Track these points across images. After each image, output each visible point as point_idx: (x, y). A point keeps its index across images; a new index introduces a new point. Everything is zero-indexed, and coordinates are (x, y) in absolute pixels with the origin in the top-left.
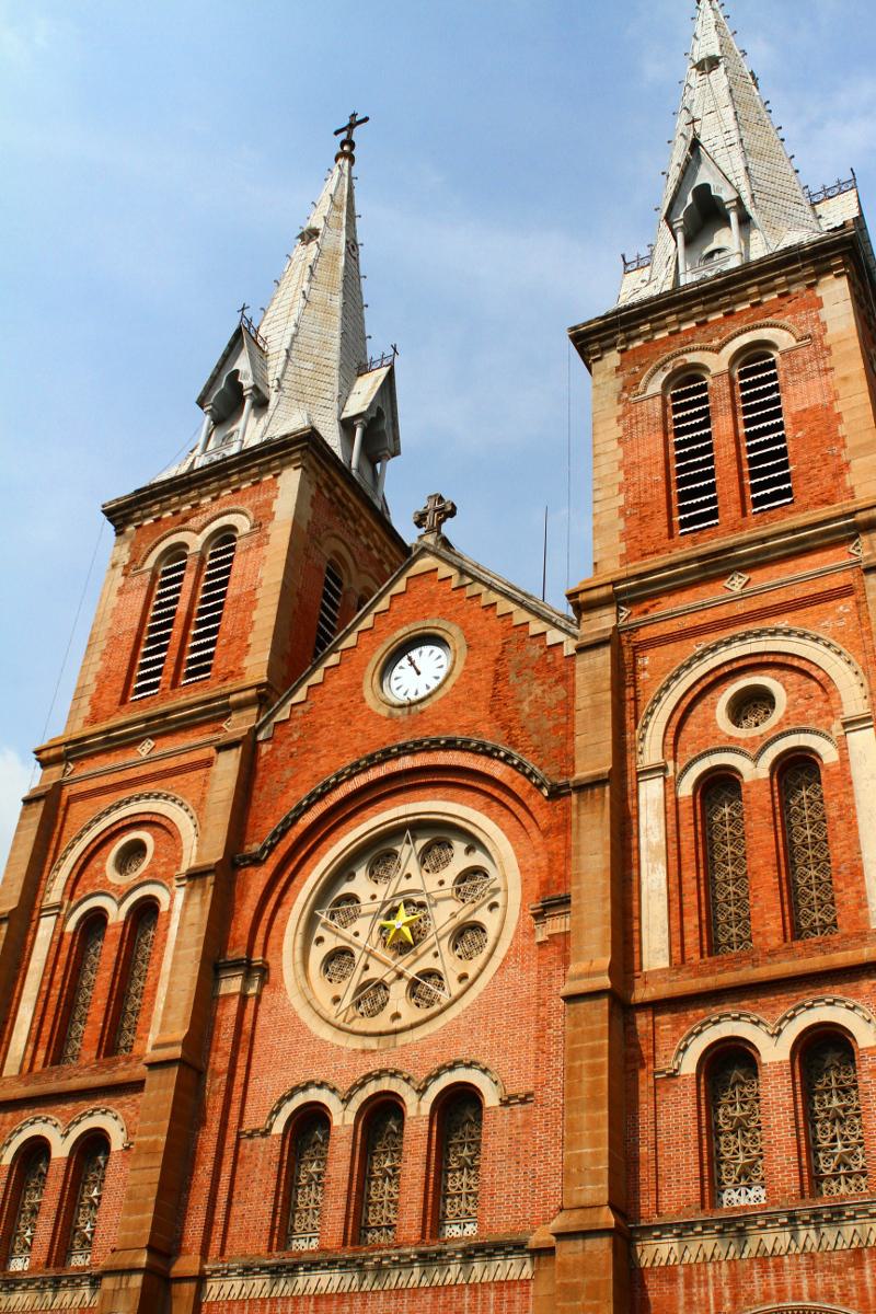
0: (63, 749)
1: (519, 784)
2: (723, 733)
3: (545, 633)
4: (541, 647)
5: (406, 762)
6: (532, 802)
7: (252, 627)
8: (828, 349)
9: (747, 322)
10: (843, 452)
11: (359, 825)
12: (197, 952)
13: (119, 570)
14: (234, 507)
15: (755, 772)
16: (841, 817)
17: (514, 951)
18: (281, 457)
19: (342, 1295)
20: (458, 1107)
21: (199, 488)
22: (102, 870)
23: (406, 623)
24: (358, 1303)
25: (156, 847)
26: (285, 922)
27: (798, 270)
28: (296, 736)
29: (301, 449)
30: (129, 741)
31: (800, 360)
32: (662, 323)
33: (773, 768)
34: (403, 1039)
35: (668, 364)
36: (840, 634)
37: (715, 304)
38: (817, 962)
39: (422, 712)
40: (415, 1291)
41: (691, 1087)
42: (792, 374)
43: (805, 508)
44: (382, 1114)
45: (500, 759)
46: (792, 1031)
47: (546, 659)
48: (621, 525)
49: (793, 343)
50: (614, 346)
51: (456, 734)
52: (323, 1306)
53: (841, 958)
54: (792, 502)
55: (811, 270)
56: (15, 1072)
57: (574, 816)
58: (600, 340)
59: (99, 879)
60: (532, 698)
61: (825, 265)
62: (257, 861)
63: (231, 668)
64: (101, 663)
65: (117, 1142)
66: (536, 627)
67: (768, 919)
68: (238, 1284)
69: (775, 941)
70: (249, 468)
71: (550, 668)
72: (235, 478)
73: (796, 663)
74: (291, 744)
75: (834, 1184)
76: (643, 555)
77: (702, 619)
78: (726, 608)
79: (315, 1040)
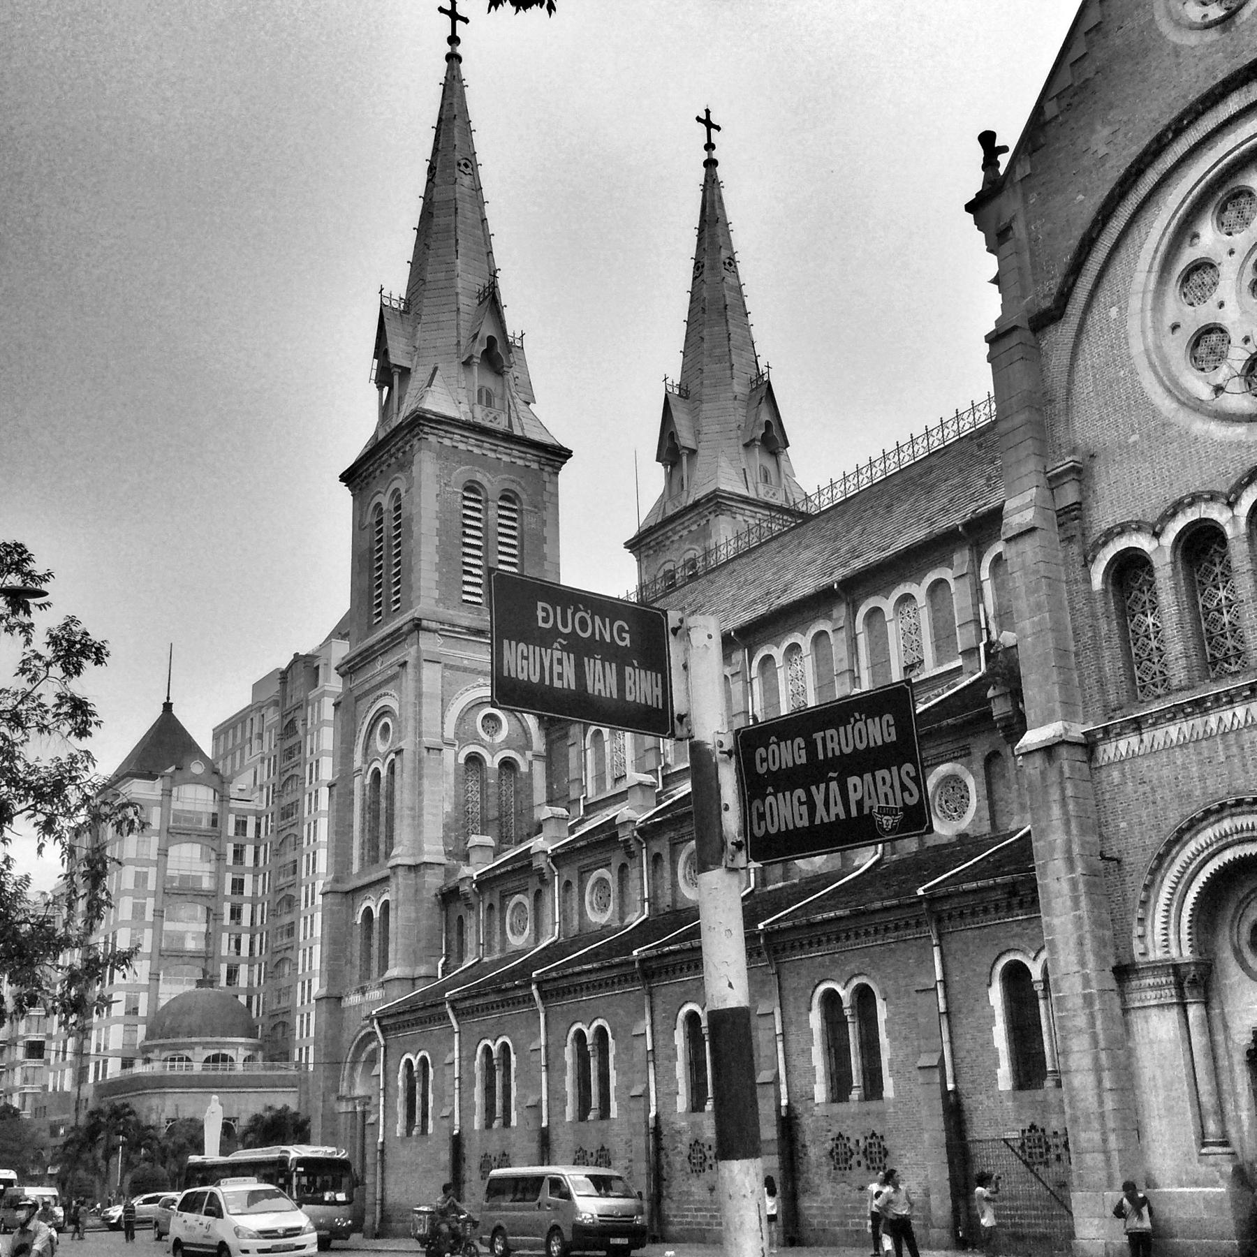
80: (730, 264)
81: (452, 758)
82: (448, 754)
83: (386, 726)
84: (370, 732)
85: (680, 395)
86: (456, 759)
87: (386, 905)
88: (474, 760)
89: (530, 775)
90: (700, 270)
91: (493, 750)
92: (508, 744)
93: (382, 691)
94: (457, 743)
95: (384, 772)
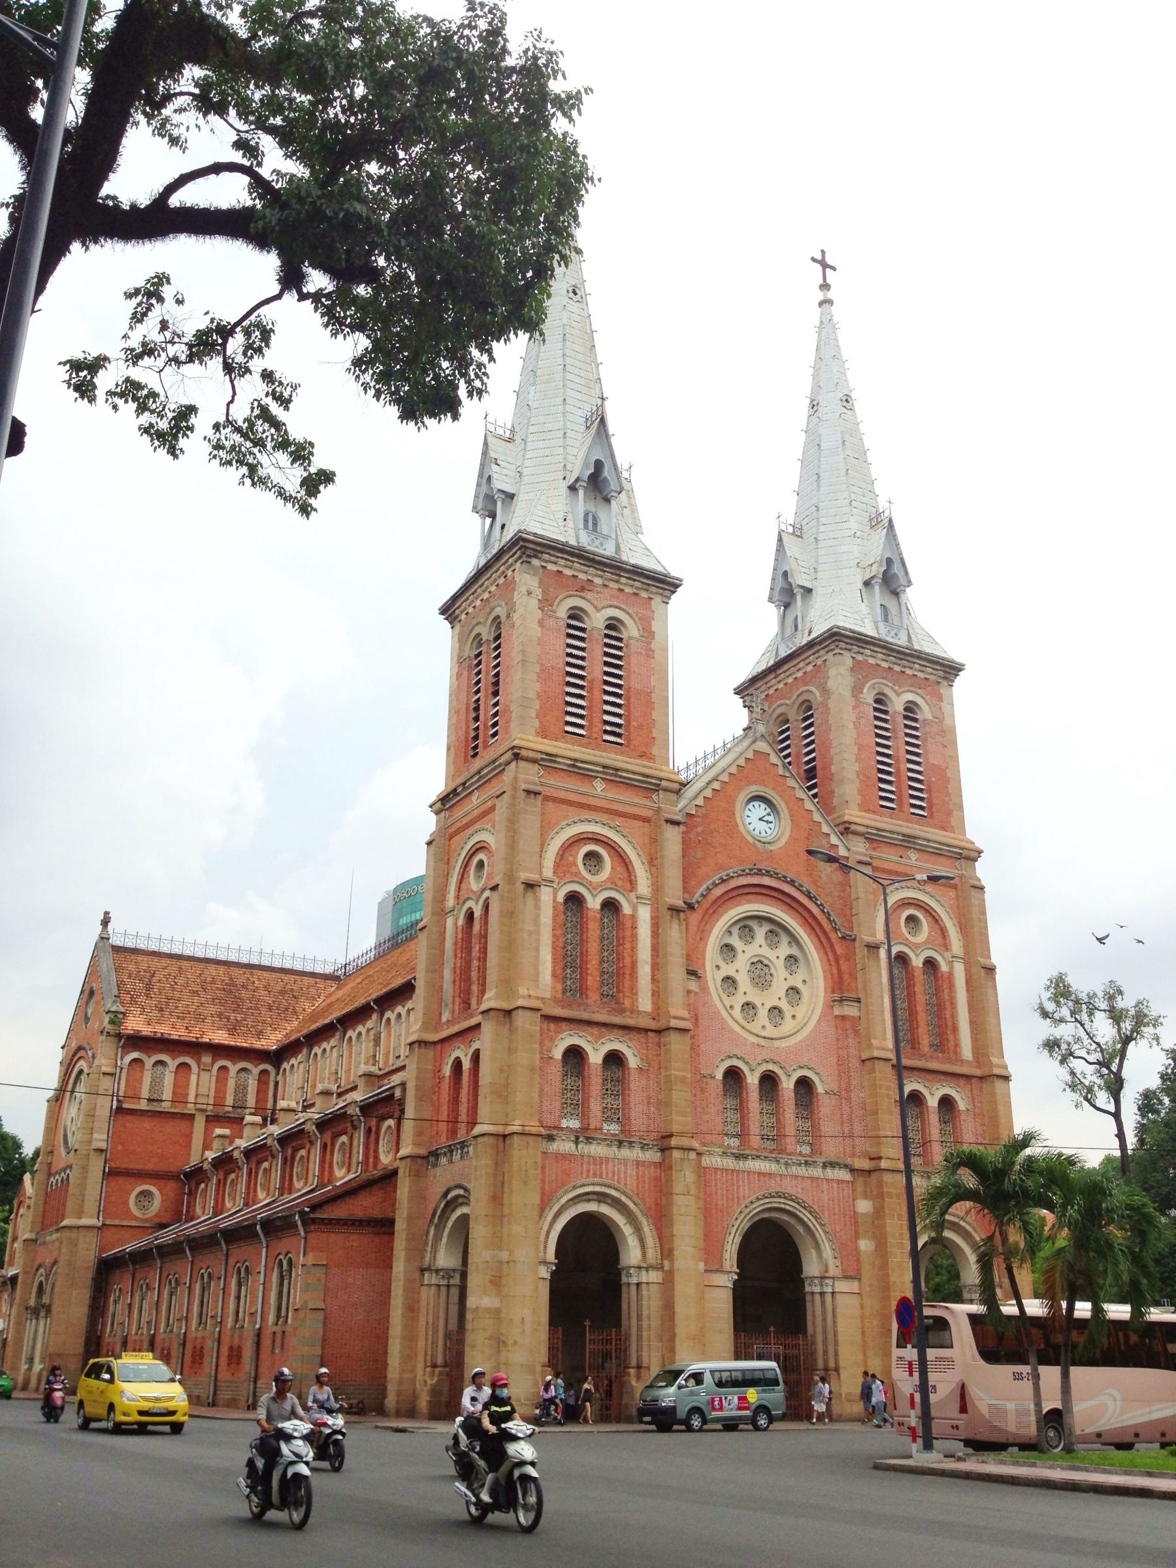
0: (540, 756)
1: (824, 922)
3: (828, 835)
5: (766, 881)
6: (832, 935)
11: (738, 905)
14: (623, 606)
17: (823, 1015)
18: (657, 587)
19: (770, 1174)
20: (804, 1085)
22: (575, 864)
23: (755, 783)
24: (778, 1179)
26: (704, 951)
28: (700, 829)
30: (588, 776)
32: (875, 654)
34: (777, 1044)
35: (876, 686)
37: (900, 662)
39: (771, 851)
40: (803, 1177)
43: (935, 826)
44: (769, 1081)
45: (816, 904)
46: (939, 1094)
48: (858, 785)
50: (850, 650)
51: (790, 876)
52: (762, 1178)
55: (941, 674)
56: (548, 995)
58: (847, 643)
59: (574, 869)
60: (825, 872)
61: (948, 676)
62: (691, 907)
63: (644, 749)
64: (538, 684)
65: (633, 1062)
66: (825, 829)
68: (719, 1160)
70: (635, 580)
72: (623, 580)
74: (697, 833)
78: (909, 868)
79: (731, 1031)
80: (847, 400)
81: (549, 899)
82: (545, 894)
83: (481, 864)
84: (466, 866)
85: (793, 534)
86: (555, 897)
87: (476, 1057)
88: (574, 899)
89: (633, 917)
90: (815, 408)
91: (593, 888)
92: (611, 883)
93: (477, 826)
94: (556, 880)
95: (478, 913)
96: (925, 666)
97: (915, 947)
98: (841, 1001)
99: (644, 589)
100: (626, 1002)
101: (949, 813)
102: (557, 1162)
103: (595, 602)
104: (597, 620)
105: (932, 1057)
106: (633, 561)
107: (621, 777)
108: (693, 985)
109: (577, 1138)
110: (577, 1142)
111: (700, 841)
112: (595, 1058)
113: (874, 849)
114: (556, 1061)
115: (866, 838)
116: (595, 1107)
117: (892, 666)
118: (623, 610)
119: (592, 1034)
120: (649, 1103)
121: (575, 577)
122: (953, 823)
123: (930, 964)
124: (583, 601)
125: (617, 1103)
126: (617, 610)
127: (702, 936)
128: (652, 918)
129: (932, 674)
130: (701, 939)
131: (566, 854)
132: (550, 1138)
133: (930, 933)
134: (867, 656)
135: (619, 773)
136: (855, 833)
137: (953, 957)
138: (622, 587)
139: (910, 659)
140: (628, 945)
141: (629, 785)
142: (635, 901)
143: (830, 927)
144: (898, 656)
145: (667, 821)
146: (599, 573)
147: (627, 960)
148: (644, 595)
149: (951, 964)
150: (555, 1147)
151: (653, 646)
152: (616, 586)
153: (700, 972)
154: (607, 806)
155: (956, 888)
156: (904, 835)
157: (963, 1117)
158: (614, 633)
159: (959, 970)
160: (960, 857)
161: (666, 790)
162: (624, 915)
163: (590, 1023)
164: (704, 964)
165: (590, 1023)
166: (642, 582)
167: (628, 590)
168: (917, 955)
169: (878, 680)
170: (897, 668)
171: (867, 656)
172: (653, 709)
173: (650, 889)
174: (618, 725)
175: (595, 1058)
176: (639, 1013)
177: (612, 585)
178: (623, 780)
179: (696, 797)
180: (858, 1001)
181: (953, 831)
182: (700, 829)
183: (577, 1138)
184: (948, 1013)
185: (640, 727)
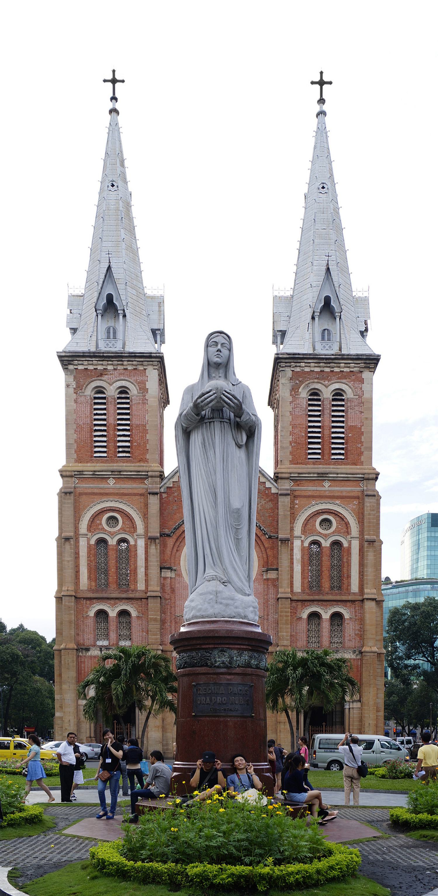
0: (73, 473)
2: (317, 530)
4: (264, 487)
6: (263, 538)
7: (148, 442)
8: (363, 403)
9: (338, 378)
10: (362, 447)
12: (157, 564)
13: (71, 390)
14: (126, 378)
15: (326, 544)
16: (346, 562)
21: (108, 361)
22: (101, 524)
25: (123, 521)
26: (180, 556)
27: (359, 364)
28: (176, 494)
29: (158, 361)
30: (104, 479)
31: (353, 404)
32: (309, 365)
33: (330, 544)
36: (353, 510)
37: (329, 365)
38: (338, 598)
41: (305, 621)
42: (351, 409)
47: (265, 491)
49: (352, 396)
50: (290, 366)
53: (344, 598)
54: (344, 459)
56: (86, 589)
57: (280, 548)
58: (286, 363)
59: (100, 527)
60: (261, 504)
62: (168, 536)
63: (141, 457)
64: (76, 435)
65: (134, 613)
67: (326, 584)
69: (327, 590)
70: (133, 361)
71: (267, 495)
72: (125, 363)
73: (340, 515)
74: (174, 496)
75: (334, 644)
76: (297, 463)
77: (316, 493)
88: (102, 541)
89: (135, 546)
91: (112, 535)
96: (350, 363)
97: (326, 536)
98: (267, 571)
99: (141, 365)
100: (132, 587)
101: (362, 453)
102: (91, 659)
103: (109, 381)
104: (112, 391)
105: (327, 594)
106: (131, 351)
107: (124, 475)
108: (168, 574)
109: (101, 649)
110: (101, 651)
111: (176, 501)
112: (113, 613)
113: (298, 485)
114: (91, 617)
115: (290, 480)
116: (113, 635)
117: (322, 369)
118: (126, 380)
119: (110, 604)
120: (143, 631)
121: (97, 369)
122: (362, 460)
123: (336, 544)
124: (102, 381)
125: (125, 632)
126: (123, 382)
127: (179, 550)
128: (146, 544)
129: (355, 367)
130: (177, 550)
131: (95, 520)
132: (87, 650)
133: (337, 527)
134: (303, 367)
135: (121, 473)
136: (282, 478)
137: (351, 538)
138: (125, 367)
139: (336, 361)
140: (133, 559)
141: (130, 478)
142: (136, 537)
143: (261, 533)
144: (327, 361)
145: (150, 494)
146: (110, 362)
147: (132, 566)
148: (141, 368)
149: (350, 543)
150: (89, 653)
151: (147, 397)
152: (122, 367)
153: (174, 568)
154: (117, 492)
155: (359, 498)
156: (318, 474)
157: (346, 622)
158: (123, 396)
159: (355, 545)
160: (364, 479)
161: (152, 477)
162: (131, 545)
163: (108, 599)
164: (179, 563)
165: (108, 599)
166: (138, 361)
167: (130, 368)
168: (326, 541)
169: (312, 381)
170: (327, 370)
171: (303, 367)
172: (147, 433)
173: (144, 530)
174: (128, 447)
175: (113, 613)
176: (137, 591)
177: (119, 367)
178: (125, 476)
179: (173, 477)
180: (277, 570)
181: (362, 463)
182: (176, 494)
183: (101, 649)
184: (345, 570)
185: (139, 445)
